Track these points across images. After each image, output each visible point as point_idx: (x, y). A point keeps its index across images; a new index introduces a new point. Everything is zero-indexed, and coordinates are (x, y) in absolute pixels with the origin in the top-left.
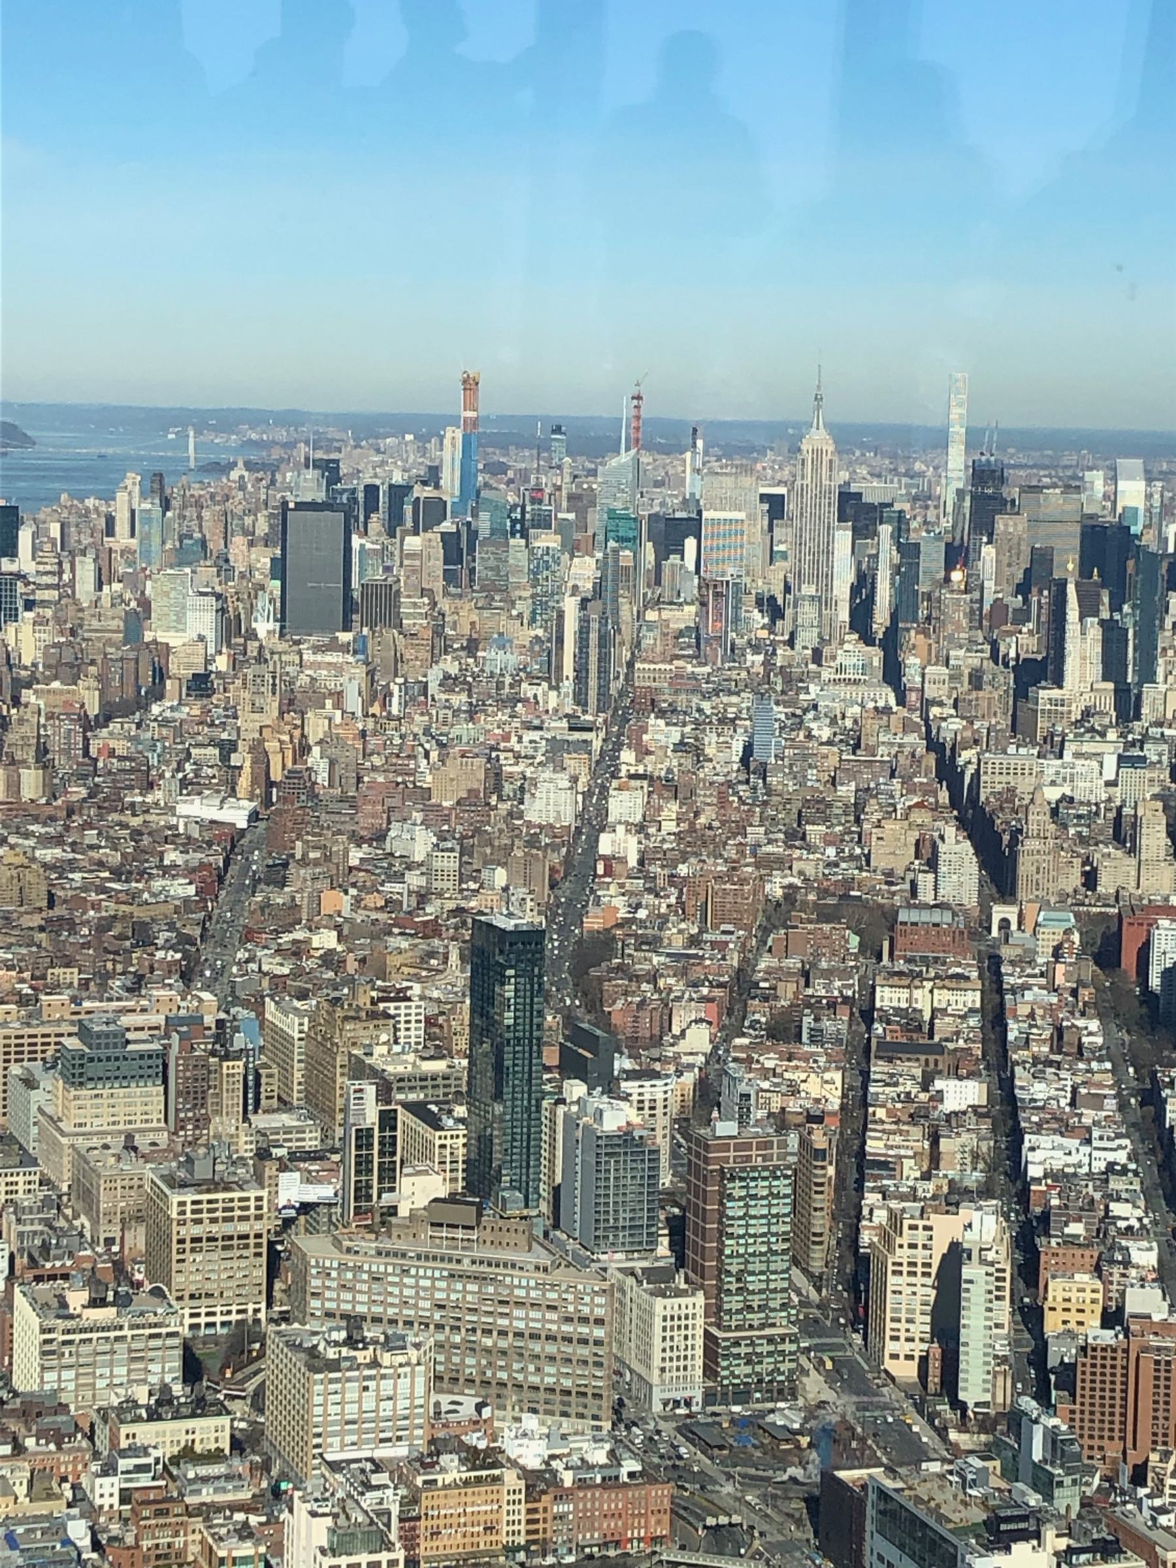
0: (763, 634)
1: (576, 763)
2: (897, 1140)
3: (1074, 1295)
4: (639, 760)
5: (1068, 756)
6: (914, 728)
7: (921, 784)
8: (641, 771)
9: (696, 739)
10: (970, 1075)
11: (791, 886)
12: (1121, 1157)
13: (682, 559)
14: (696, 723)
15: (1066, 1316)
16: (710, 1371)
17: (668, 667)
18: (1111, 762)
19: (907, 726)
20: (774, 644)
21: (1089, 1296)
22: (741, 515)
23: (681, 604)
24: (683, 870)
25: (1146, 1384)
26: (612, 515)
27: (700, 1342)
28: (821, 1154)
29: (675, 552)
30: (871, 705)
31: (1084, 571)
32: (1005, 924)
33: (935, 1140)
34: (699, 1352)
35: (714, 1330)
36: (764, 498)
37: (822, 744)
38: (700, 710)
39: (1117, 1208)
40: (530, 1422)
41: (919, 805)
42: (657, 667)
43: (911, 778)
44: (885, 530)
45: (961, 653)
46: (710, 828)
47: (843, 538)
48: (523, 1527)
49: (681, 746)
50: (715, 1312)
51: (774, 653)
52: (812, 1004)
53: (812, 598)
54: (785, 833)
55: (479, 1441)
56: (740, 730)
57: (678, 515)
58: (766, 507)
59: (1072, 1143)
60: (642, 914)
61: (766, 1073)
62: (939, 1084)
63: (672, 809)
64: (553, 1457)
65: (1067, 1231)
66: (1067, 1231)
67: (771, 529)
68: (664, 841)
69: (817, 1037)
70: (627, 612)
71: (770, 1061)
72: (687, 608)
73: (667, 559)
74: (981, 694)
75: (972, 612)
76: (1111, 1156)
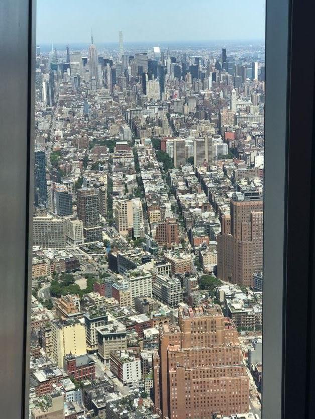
1: (48, 117)
2: (118, 188)
3: (155, 215)
5: (148, 109)
10: (133, 173)
12: (163, 187)
15: (154, 219)
16: (85, 236)
18: (156, 109)
19: (115, 105)
20: (87, 89)
21: (158, 214)
22: (79, 63)
23: (67, 83)
24: (72, 137)
25: (170, 231)
26: (51, 63)
27: (82, 231)
28: (104, 192)
30: (108, 101)
31: (149, 70)
32: (138, 143)
33: (126, 187)
34: (83, 233)
35: (85, 228)
36: (83, 59)
38: (73, 105)
39: (162, 197)
40: (50, 249)
44: (108, 65)
45: (125, 89)
47: (100, 67)
48: (50, 270)
49: (70, 112)
50: (85, 225)
52: (100, 162)
53: (94, 80)
55: (39, 254)
59: (153, 185)
60: (65, 147)
61: (92, 177)
62: (126, 176)
63: (69, 125)
64: (55, 256)
65: (153, 202)
66: (153, 202)
69: (102, 169)
70: (56, 85)
71: (93, 174)
76: (161, 187)
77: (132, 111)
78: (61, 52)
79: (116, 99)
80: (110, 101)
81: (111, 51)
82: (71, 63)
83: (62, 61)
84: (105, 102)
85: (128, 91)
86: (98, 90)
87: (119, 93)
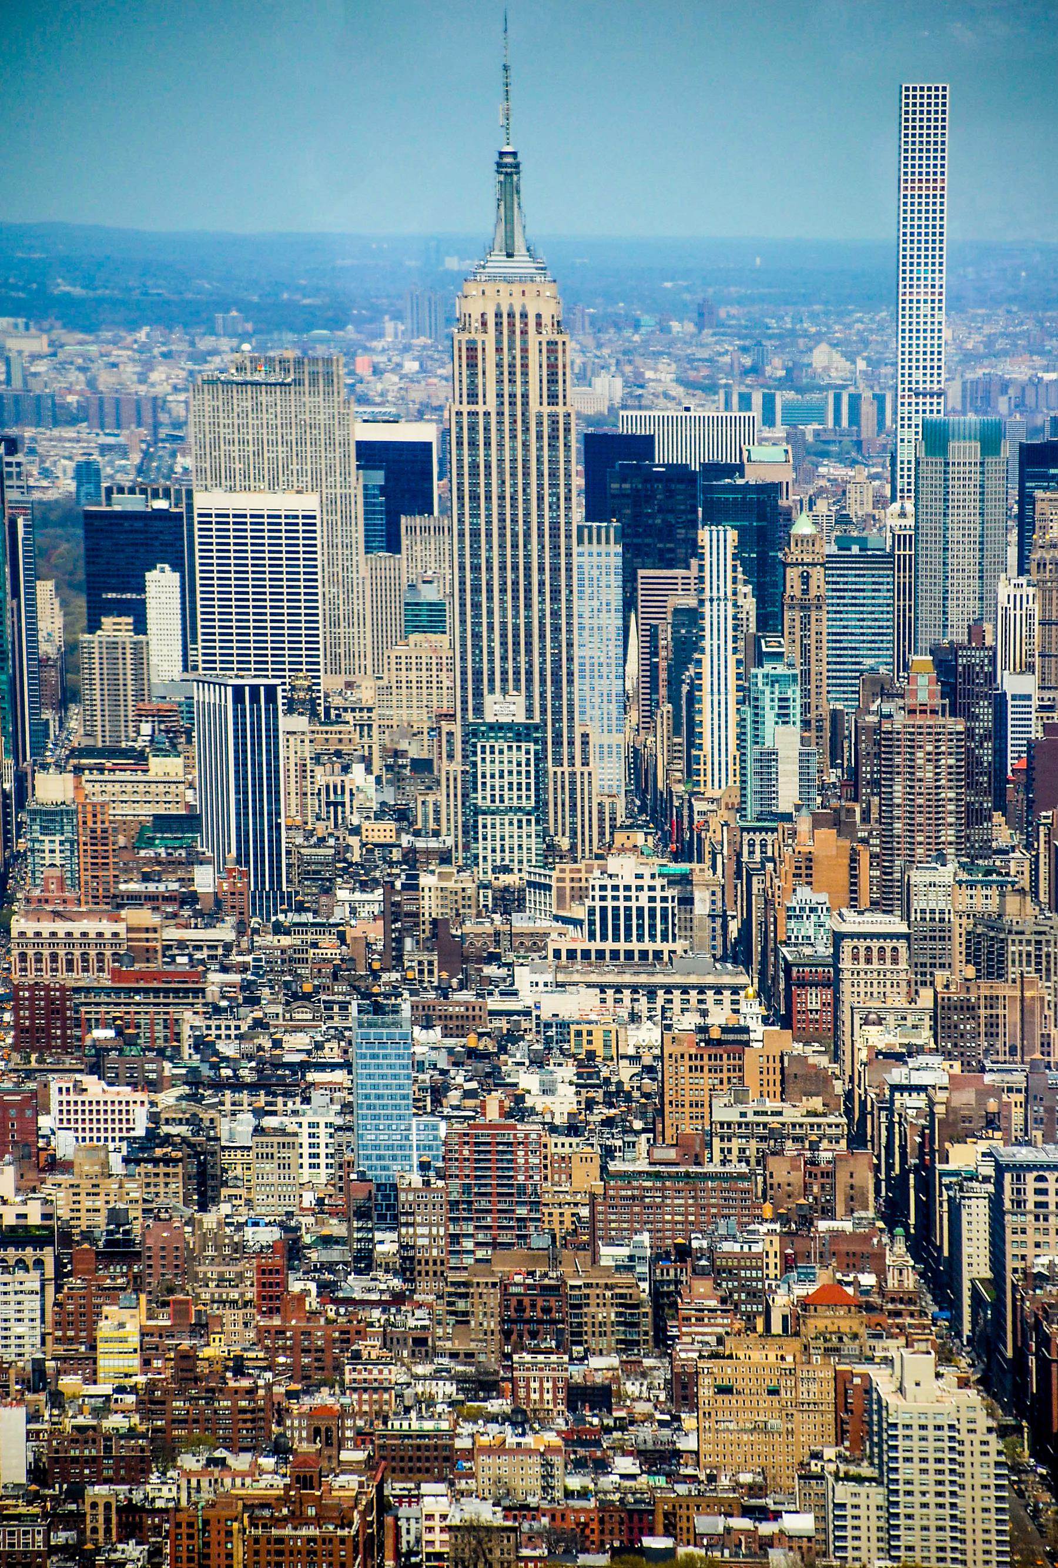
0: (382, 831)
4: (26, 1189)
6: (818, 1082)
7: (837, 1235)
8: (35, 1219)
9: (194, 1121)
11: (471, 1529)
13: (140, 626)
14: (193, 1079)
17: (107, 927)
20: (412, 859)
23: (141, 757)
29: (120, 608)
30: (690, 1021)
37: (553, 1129)
38: (201, 1044)
41: (830, 1297)
42: (76, 927)
43: (807, 1221)
45: (947, 873)
46: (239, 1370)
51: (412, 886)
54: (460, 1380)
56: (315, 1095)
57: (124, 503)
58: (378, 477)
67: (393, 545)
68: (102, 1411)
72: (158, 766)
73: (94, 626)
74: (1004, 990)
75: (972, 761)
77: (1020, 1170)
78: (74, 343)
79: (813, 1000)
80: (719, 1017)
81: (775, 368)
82: (203, 501)
83: (86, 473)
84: (648, 1034)
85: (985, 901)
86: (560, 874)
87: (853, 922)
